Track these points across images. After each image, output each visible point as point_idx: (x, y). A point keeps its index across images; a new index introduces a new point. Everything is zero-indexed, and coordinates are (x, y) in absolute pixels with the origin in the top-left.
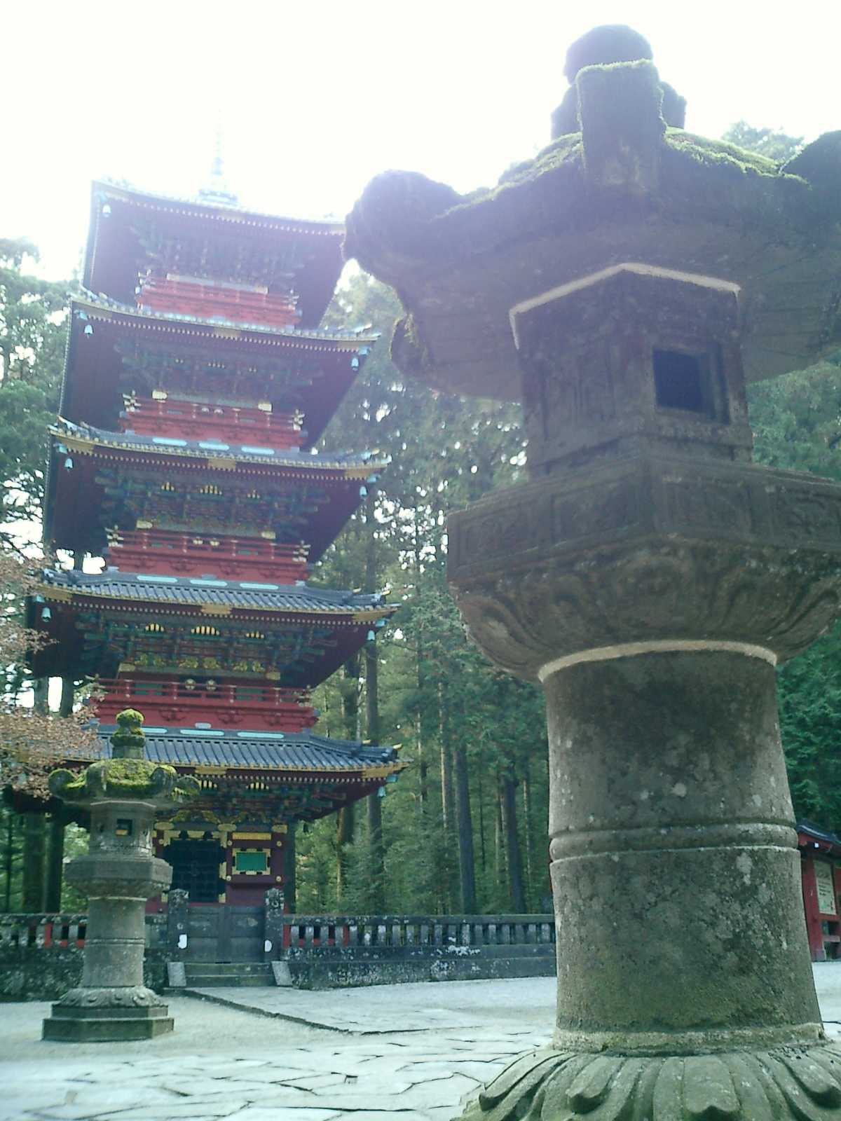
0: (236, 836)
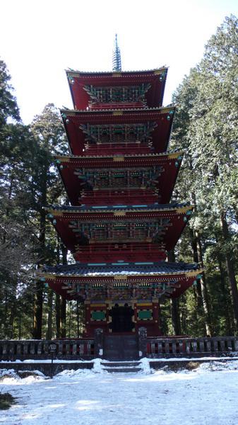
0: (138, 305)
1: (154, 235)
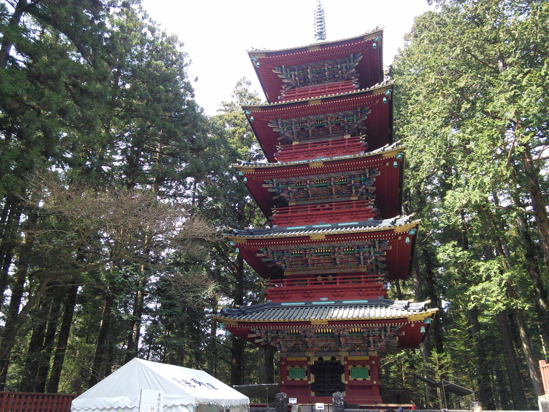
0: (349, 358)
1: (369, 261)
